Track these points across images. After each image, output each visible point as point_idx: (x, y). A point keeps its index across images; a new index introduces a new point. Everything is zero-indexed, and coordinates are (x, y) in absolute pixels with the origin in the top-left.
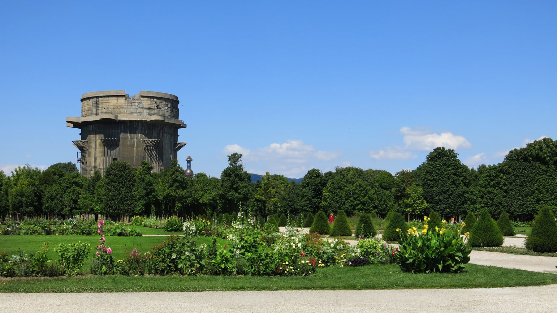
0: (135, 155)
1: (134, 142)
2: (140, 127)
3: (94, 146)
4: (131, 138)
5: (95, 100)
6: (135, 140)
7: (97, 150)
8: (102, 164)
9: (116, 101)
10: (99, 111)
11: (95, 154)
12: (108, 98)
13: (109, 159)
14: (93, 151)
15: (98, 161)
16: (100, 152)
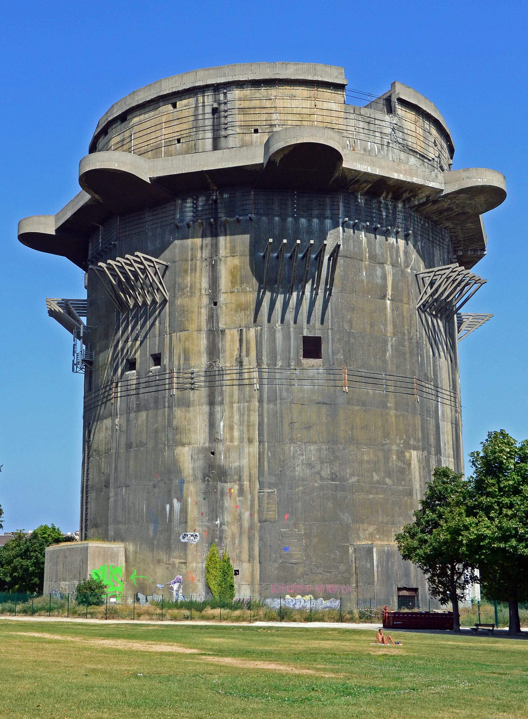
0: (390, 328)
1: (384, 277)
2: (400, 216)
3: (205, 283)
4: (373, 257)
5: (209, 99)
6: (388, 268)
7: (222, 298)
8: (250, 361)
9: (308, 104)
10: (231, 142)
11: (212, 318)
12: (273, 92)
13: (287, 337)
14: (198, 307)
15: (230, 344)
16: (240, 308)
